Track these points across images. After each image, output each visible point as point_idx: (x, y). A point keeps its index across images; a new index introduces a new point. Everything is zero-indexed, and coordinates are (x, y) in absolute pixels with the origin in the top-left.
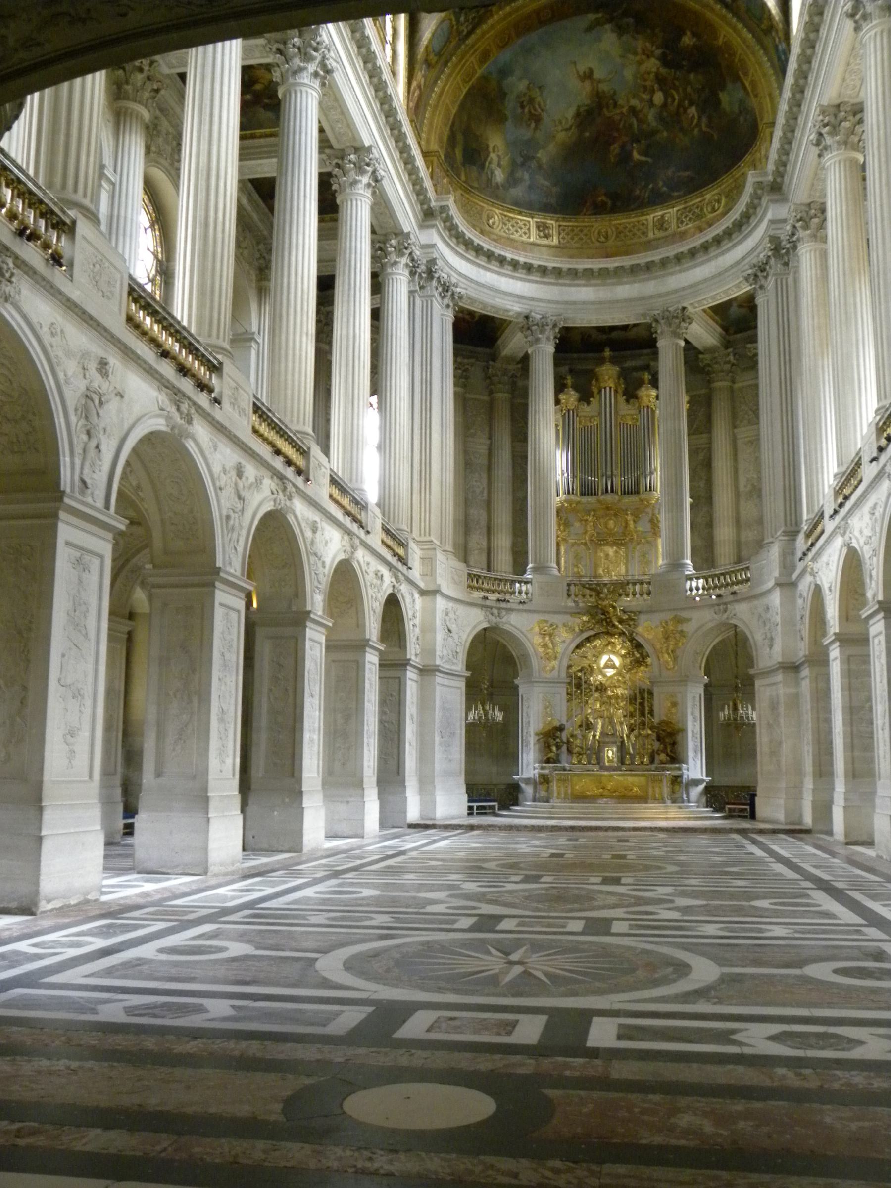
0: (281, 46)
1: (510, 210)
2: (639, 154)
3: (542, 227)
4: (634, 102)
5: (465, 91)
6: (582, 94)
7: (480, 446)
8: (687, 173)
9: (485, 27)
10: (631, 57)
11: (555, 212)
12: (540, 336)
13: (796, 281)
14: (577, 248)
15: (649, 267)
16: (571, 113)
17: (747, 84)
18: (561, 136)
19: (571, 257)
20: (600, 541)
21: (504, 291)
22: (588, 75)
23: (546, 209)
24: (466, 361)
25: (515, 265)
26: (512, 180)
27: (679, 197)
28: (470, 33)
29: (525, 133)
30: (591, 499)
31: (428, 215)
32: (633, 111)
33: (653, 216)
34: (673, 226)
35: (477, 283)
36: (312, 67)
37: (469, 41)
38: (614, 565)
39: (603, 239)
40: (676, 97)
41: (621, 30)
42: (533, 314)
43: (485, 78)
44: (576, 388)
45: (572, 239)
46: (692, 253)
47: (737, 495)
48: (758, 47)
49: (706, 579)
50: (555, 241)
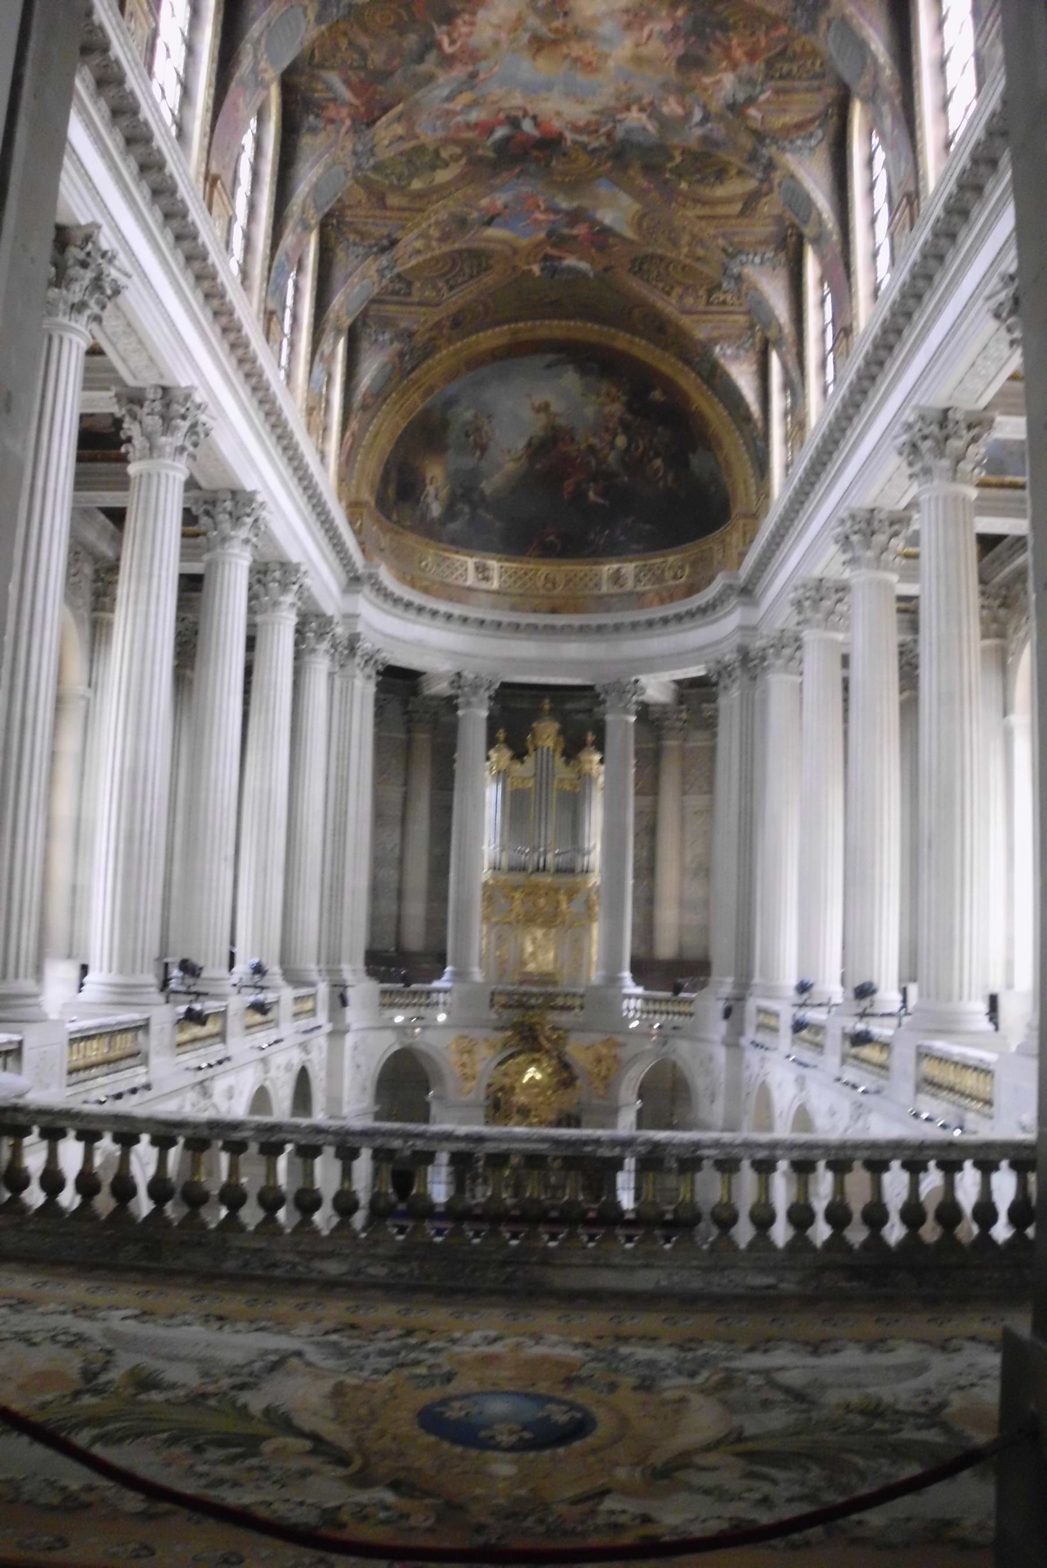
0: (210, 508)
1: (445, 550)
2: (596, 493)
3: (482, 570)
4: (592, 440)
5: (403, 426)
6: (535, 426)
7: (395, 794)
8: (648, 527)
9: (430, 362)
10: (594, 398)
11: (498, 552)
12: (473, 699)
13: (764, 701)
14: (521, 595)
15: (600, 629)
16: (521, 444)
17: (721, 459)
18: (510, 466)
19: (514, 608)
20: (529, 920)
21: (432, 644)
22: (545, 408)
23: (486, 547)
24: (382, 696)
25: (449, 617)
26: (450, 512)
27: (638, 551)
28: (413, 369)
29: (468, 462)
30: (518, 878)
31: (354, 581)
32: (591, 449)
33: (607, 569)
34: (630, 584)
35: (404, 641)
36: (243, 533)
37: (413, 375)
38: (539, 952)
39: (549, 586)
40: (641, 444)
41: (583, 371)
42: (465, 673)
43: (427, 412)
44: (509, 743)
45: (515, 582)
46: (650, 624)
47: (683, 870)
48: (733, 427)
49: (646, 1000)
50: (495, 585)
